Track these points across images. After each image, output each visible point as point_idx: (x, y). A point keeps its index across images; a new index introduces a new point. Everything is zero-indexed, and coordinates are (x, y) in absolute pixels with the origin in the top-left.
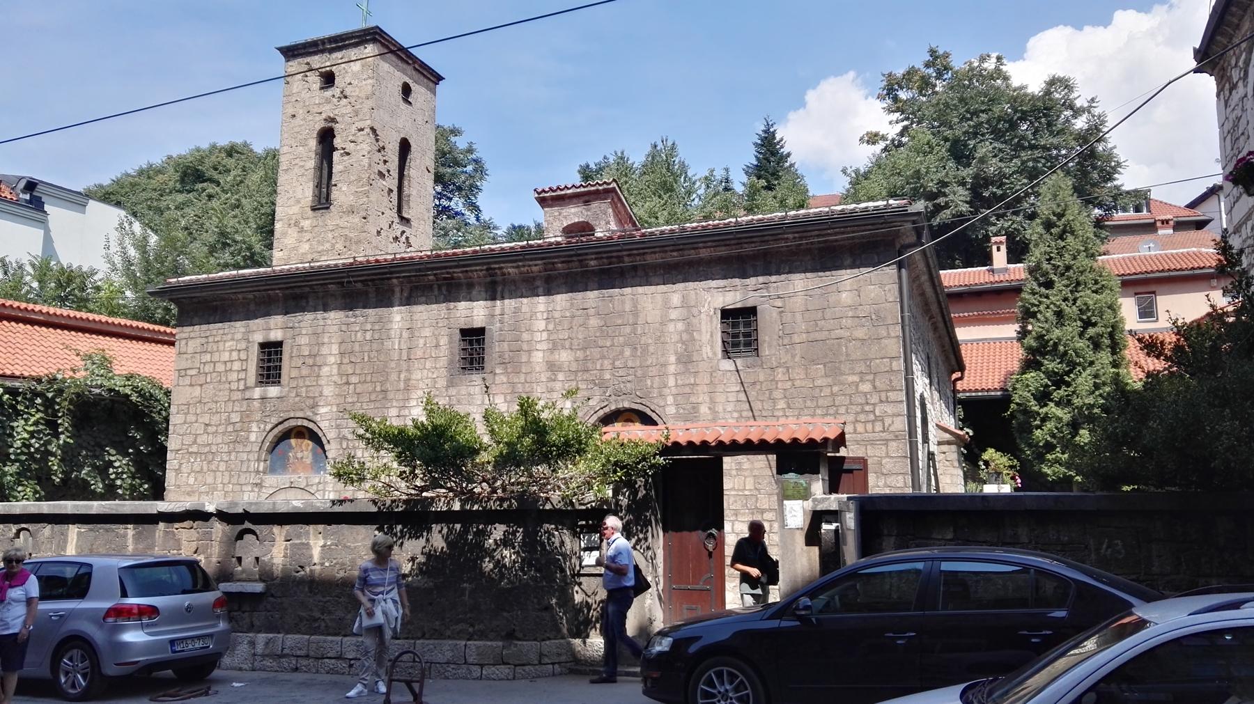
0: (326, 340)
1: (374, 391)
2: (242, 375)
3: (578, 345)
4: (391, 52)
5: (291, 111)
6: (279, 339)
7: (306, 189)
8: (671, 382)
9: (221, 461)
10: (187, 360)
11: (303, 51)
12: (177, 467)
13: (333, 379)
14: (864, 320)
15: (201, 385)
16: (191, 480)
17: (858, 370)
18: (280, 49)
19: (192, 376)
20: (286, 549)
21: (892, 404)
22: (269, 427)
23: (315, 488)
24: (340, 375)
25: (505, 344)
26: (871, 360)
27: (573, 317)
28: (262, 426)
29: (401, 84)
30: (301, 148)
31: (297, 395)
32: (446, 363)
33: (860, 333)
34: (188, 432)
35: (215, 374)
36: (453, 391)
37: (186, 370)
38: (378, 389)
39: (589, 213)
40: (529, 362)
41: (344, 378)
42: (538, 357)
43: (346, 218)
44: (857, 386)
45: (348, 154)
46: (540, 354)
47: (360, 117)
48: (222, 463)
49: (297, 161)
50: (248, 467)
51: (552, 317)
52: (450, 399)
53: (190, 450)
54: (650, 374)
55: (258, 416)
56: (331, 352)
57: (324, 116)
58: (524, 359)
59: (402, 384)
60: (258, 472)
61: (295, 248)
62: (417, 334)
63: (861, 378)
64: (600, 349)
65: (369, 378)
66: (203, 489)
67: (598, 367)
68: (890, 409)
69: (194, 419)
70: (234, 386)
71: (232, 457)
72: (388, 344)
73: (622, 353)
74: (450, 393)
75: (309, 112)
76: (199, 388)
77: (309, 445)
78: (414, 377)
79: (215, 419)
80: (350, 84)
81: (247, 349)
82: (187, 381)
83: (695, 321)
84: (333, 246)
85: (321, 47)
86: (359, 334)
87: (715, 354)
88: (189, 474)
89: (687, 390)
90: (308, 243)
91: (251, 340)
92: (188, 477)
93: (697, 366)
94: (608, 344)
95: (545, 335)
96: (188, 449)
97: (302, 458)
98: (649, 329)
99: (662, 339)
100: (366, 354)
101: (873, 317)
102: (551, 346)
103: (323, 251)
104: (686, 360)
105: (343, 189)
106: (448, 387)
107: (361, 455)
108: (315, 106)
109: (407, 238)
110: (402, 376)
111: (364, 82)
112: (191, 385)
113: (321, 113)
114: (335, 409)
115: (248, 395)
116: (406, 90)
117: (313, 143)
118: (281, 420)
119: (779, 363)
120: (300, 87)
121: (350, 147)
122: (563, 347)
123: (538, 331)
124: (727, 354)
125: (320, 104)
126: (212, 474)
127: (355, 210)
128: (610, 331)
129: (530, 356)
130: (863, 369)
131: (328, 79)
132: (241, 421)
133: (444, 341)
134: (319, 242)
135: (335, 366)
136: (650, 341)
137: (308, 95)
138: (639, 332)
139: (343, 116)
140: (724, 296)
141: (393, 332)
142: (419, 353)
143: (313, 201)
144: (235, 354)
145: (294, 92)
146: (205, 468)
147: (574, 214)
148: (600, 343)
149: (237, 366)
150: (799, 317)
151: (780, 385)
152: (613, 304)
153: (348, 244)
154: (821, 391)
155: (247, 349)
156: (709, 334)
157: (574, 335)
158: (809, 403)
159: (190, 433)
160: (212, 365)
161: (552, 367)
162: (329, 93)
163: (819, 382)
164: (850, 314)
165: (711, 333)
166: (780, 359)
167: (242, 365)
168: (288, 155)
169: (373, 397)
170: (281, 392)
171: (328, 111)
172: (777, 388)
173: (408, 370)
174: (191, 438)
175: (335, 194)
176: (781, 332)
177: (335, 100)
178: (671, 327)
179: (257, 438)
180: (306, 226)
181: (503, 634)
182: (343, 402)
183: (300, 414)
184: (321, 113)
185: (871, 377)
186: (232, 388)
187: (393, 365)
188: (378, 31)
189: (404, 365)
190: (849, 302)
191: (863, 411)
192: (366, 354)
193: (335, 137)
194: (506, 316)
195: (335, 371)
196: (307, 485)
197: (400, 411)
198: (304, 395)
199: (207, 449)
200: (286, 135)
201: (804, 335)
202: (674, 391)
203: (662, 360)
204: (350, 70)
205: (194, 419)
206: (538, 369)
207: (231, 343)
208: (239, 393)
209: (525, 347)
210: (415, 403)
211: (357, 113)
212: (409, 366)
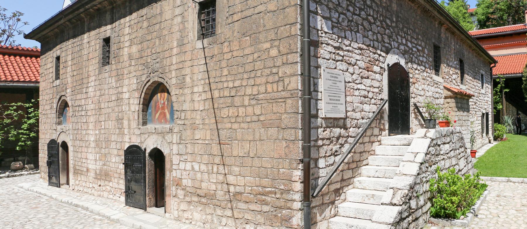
21: (290, 66)
68: (288, 70)
87: (194, 36)
191: (272, 74)
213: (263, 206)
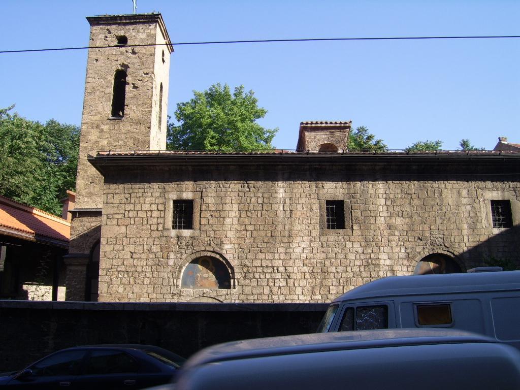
5: (95, 57)
7: (105, 106)
15: (127, 226)
16: (121, 290)
18: (88, 19)
19: (118, 219)
23: (223, 297)
24: (240, 224)
28: (179, 256)
30: (102, 80)
34: (117, 256)
36: (324, 239)
37: (113, 214)
43: (134, 126)
46: (383, 219)
47: (146, 65)
48: (146, 279)
49: (99, 88)
53: (119, 269)
57: (119, 62)
58: (372, 221)
61: (96, 142)
65: (262, 228)
69: (121, 248)
70: (154, 227)
72: (275, 207)
79: (139, 249)
82: (114, 222)
84: (125, 143)
88: (119, 285)
94: (426, 215)
102: (389, 214)
105: (134, 108)
107: (258, 277)
108: (113, 56)
110: (287, 227)
114: (236, 246)
117: (112, 79)
121: (138, 84)
133: (316, 207)
134: (115, 140)
136: (451, 215)
139: (133, 64)
144: (154, 207)
149: (155, 214)
153: (136, 143)
160: (135, 212)
161: (390, 227)
162: (123, 49)
168: (92, 83)
170: (194, 233)
171: (122, 60)
173: (291, 224)
178: (463, 208)
183: (208, 249)
186: (152, 228)
188: (160, 16)
195: (236, 221)
196: (217, 295)
198: (212, 236)
199: (133, 269)
200: (90, 71)
204: (138, 37)
205: (121, 248)
207: (150, 199)
209: (372, 214)
211: (143, 64)
212: (291, 221)
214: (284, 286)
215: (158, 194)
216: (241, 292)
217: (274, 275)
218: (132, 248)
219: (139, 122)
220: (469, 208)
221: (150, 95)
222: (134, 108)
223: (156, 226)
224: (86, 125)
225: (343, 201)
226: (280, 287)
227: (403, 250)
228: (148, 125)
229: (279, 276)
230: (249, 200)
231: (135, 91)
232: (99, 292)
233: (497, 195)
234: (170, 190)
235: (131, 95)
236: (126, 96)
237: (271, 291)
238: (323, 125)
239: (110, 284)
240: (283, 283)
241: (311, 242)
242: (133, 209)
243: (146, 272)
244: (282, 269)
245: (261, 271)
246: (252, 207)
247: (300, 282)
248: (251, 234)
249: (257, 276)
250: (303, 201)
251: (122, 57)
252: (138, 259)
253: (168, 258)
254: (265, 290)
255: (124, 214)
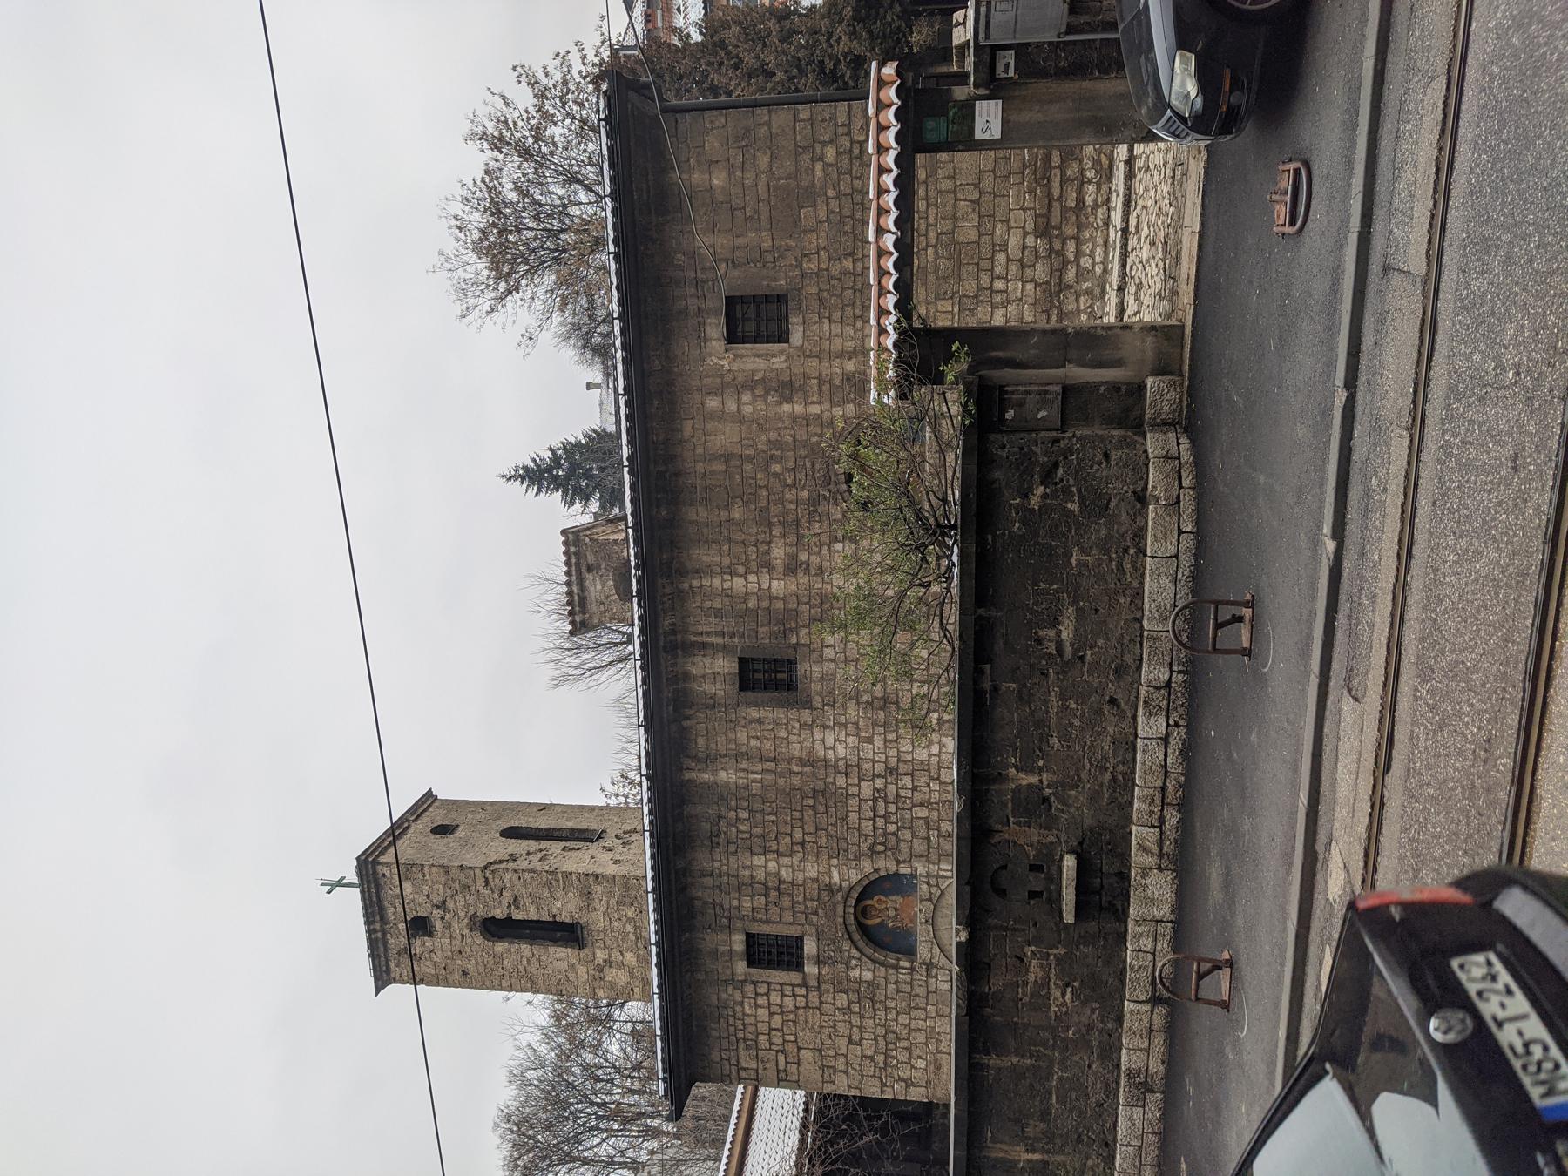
0: (747, 873)
1: (813, 807)
2: (788, 990)
3: (765, 533)
4: (394, 843)
5: (457, 976)
6: (743, 937)
7: (558, 957)
8: (815, 409)
9: (896, 1020)
10: (765, 1069)
11: (382, 959)
12: (903, 1084)
13: (796, 863)
14: (747, 156)
15: (799, 1049)
16: (921, 1064)
17: (808, 164)
19: (787, 1063)
20: (1018, 824)
21: (852, 118)
22: (855, 953)
23: (934, 890)
25: (761, 630)
26: (797, 146)
27: (730, 540)
29: (432, 836)
30: (505, 962)
31: (816, 913)
32: (781, 710)
33: (763, 161)
34: (858, 1068)
35: (785, 1029)
36: (817, 702)
37: (778, 1071)
38: (811, 802)
39: (603, 566)
40: (784, 599)
41: (796, 848)
42: (778, 587)
43: (596, 904)
44: (829, 165)
45: (516, 899)
46: (775, 583)
47: (469, 881)
48: (900, 1020)
50: (906, 983)
51: (729, 567)
52: (827, 705)
53: (882, 1065)
54: (805, 438)
55: (841, 968)
56: (762, 866)
57: (466, 932)
58: (780, 605)
59: (805, 769)
60: (912, 969)
61: (631, 972)
62: (744, 749)
63: (818, 160)
64: (771, 504)
66: (932, 1047)
67: (793, 506)
69: (841, 1060)
70: (801, 1002)
71: (892, 1004)
72: (755, 788)
73: (776, 475)
74: (819, 705)
75: (460, 952)
76: (802, 1052)
77: (880, 900)
78: (797, 753)
79: (843, 1029)
80: (428, 896)
81: (755, 983)
82: (793, 1068)
83: (740, 378)
84: (630, 920)
85: (379, 935)
86: (742, 828)
87: (782, 352)
88: (912, 1067)
89: (826, 388)
90: (626, 954)
91: (743, 977)
92: (916, 1068)
93: (796, 375)
95: (752, 578)
96: (881, 1069)
97: (896, 909)
98: (748, 439)
99: (761, 421)
100: (767, 818)
101: (744, 143)
102: (765, 570)
103: (635, 933)
104: (787, 389)
105: (559, 904)
106: (812, 708)
108: (454, 943)
109: (625, 833)
110: (796, 769)
111: (427, 877)
112: (798, 1064)
113: (463, 935)
114: (835, 862)
115: (813, 983)
116: (443, 830)
117: (500, 947)
118: (846, 936)
119: (796, 266)
120: (428, 963)
122: (768, 552)
123: (746, 586)
124: (782, 336)
125: (451, 938)
126: (913, 1034)
127: (586, 891)
128: (749, 491)
129: (777, 598)
130: (807, 157)
131: (421, 926)
132: (846, 993)
133: (754, 713)
134: (623, 940)
135: (781, 860)
136: (764, 438)
137: (439, 953)
138: (751, 452)
139: (467, 906)
140: (710, 339)
141: (741, 781)
142: (768, 746)
143: (573, 947)
144: (761, 1001)
145: (433, 972)
146: (905, 1044)
147: (603, 585)
148: (764, 504)
149: (775, 998)
150: (741, 241)
151: (824, 266)
152: (716, 486)
153: (628, 900)
154: (833, 212)
155: (755, 983)
156: (757, 359)
157: (753, 539)
158: (848, 228)
159: (860, 1065)
160: (774, 1032)
161: (792, 568)
162: (438, 925)
163: (822, 215)
164: (739, 174)
165: (757, 360)
166: (791, 265)
167: (775, 990)
168: (513, 981)
169: (821, 809)
170: (811, 935)
172: (827, 270)
174: (867, 1062)
175: (565, 917)
176: (758, 265)
177: (448, 916)
178: (747, 409)
179: (869, 970)
180: (603, 956)
181: (1138, 506)
182: (826, 850)
184: (463, 935)
185: (818, 147)
186: (803, 1004)
187: (781, 781)
188: (363, 858)
189: (784, 765)
190: (724, 175)
192: (767, 818)
193: (493, 917)
194: (725, 629)
197: (840, 773)
198: (816, 903)
199: (881, 1041)
200: (488, 983)
201: (764, 234)
202: (826, 406)
203: (787, 423)
204: (411, 897)
205: (841, 1060)
206: (793, 587)
207: (747, 1007)
208: (810, 995)
209: (765, 604)
210: (831, 752)
211: (465, 887)
213: (1053, 164)
214: (912, 780)
215: (738, 994)
216: (924, 859)
217: (891, 799)
218: (842, 1043)
219: (587, 895)
220: (746, 398)
221: (531, 874)
222: (559, 904)
223: (798, 998)
224: (597, 991)
225: (739, 658)
226: (914, 789)
227: (839, 546)
228: (591, 879)
229: (892, 789)
230: (745, 836)
231: (525, 900)
232: (926, 1100)
233: (715, 329)
234: (728, 972)
235: (532, 909)
236: (536, 918)
237: (921, 805)
238: (575, 589)
239: (909, 1083)
240: (907, 781)
241: (824, 727)
242: (767, 1037)
243: (886, 1020)
244: (879, 783)
245: (882, 820)
246: (758, 831)
247: (904, 749)
248: (811, 833)
249: (892, 828)
250: (742, 735)
251: (455, 926)
252: (861, 1032)
253: (859, 981)
254: (919, 815)
255: (777, 1051)
